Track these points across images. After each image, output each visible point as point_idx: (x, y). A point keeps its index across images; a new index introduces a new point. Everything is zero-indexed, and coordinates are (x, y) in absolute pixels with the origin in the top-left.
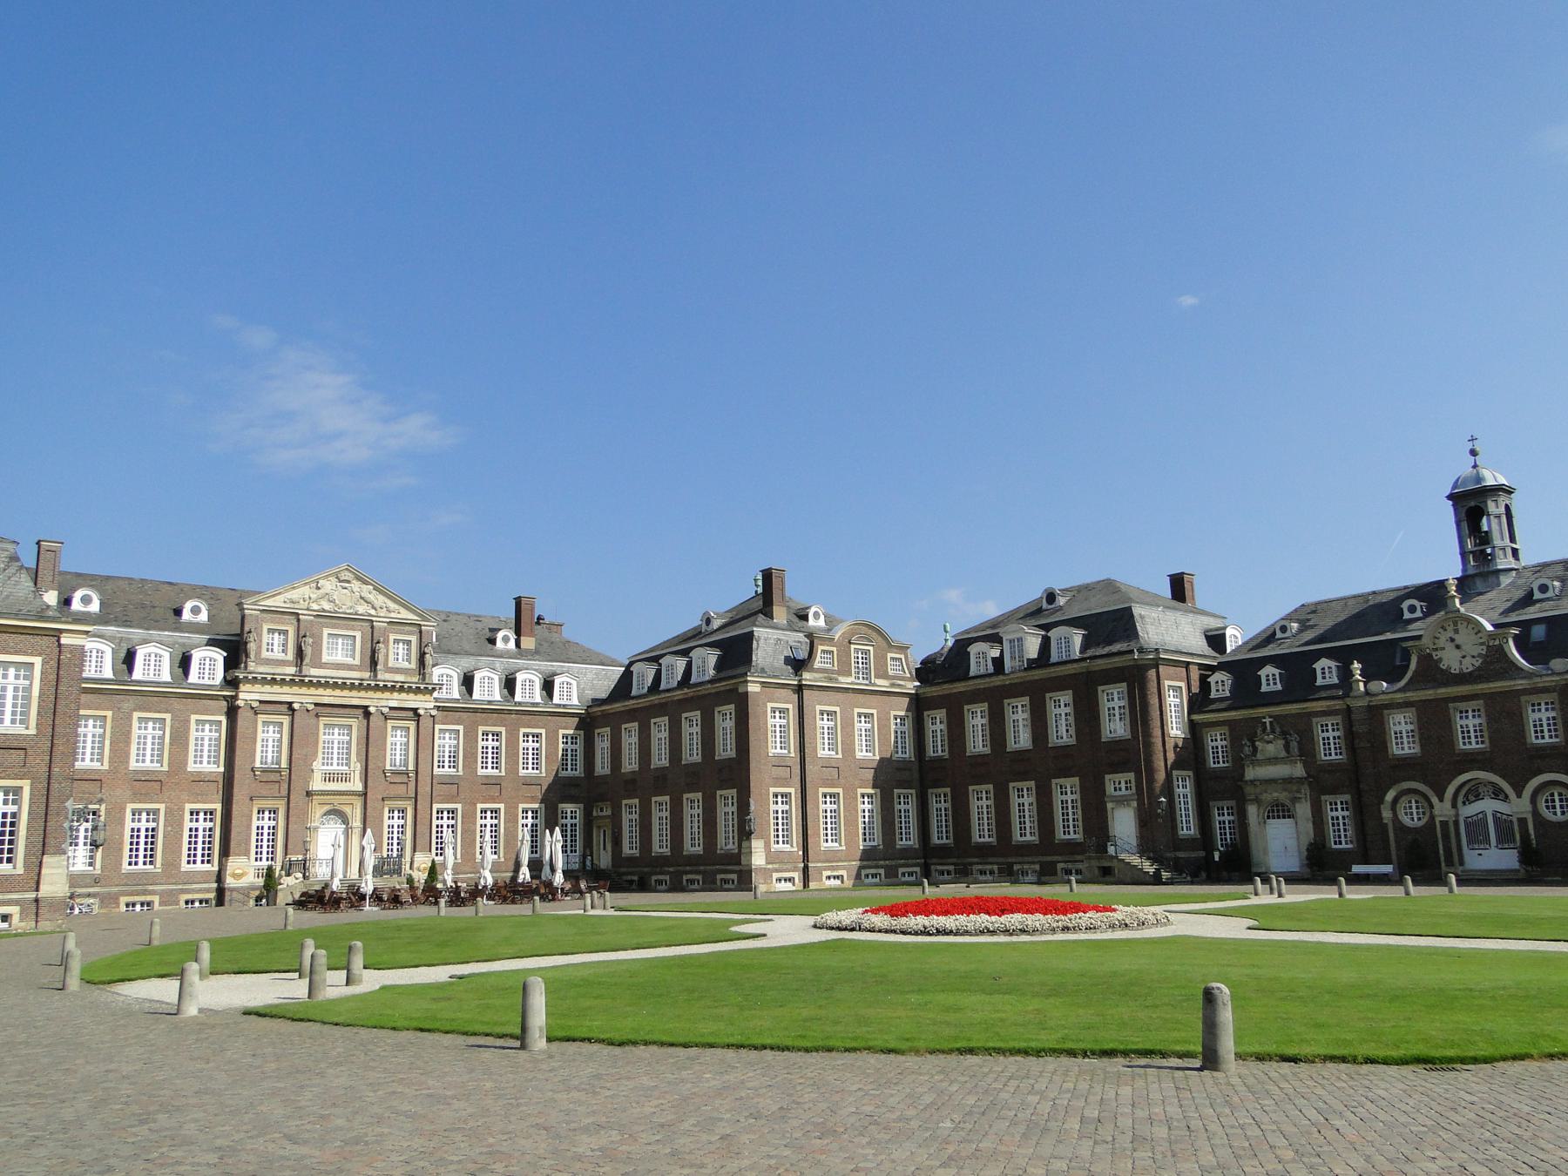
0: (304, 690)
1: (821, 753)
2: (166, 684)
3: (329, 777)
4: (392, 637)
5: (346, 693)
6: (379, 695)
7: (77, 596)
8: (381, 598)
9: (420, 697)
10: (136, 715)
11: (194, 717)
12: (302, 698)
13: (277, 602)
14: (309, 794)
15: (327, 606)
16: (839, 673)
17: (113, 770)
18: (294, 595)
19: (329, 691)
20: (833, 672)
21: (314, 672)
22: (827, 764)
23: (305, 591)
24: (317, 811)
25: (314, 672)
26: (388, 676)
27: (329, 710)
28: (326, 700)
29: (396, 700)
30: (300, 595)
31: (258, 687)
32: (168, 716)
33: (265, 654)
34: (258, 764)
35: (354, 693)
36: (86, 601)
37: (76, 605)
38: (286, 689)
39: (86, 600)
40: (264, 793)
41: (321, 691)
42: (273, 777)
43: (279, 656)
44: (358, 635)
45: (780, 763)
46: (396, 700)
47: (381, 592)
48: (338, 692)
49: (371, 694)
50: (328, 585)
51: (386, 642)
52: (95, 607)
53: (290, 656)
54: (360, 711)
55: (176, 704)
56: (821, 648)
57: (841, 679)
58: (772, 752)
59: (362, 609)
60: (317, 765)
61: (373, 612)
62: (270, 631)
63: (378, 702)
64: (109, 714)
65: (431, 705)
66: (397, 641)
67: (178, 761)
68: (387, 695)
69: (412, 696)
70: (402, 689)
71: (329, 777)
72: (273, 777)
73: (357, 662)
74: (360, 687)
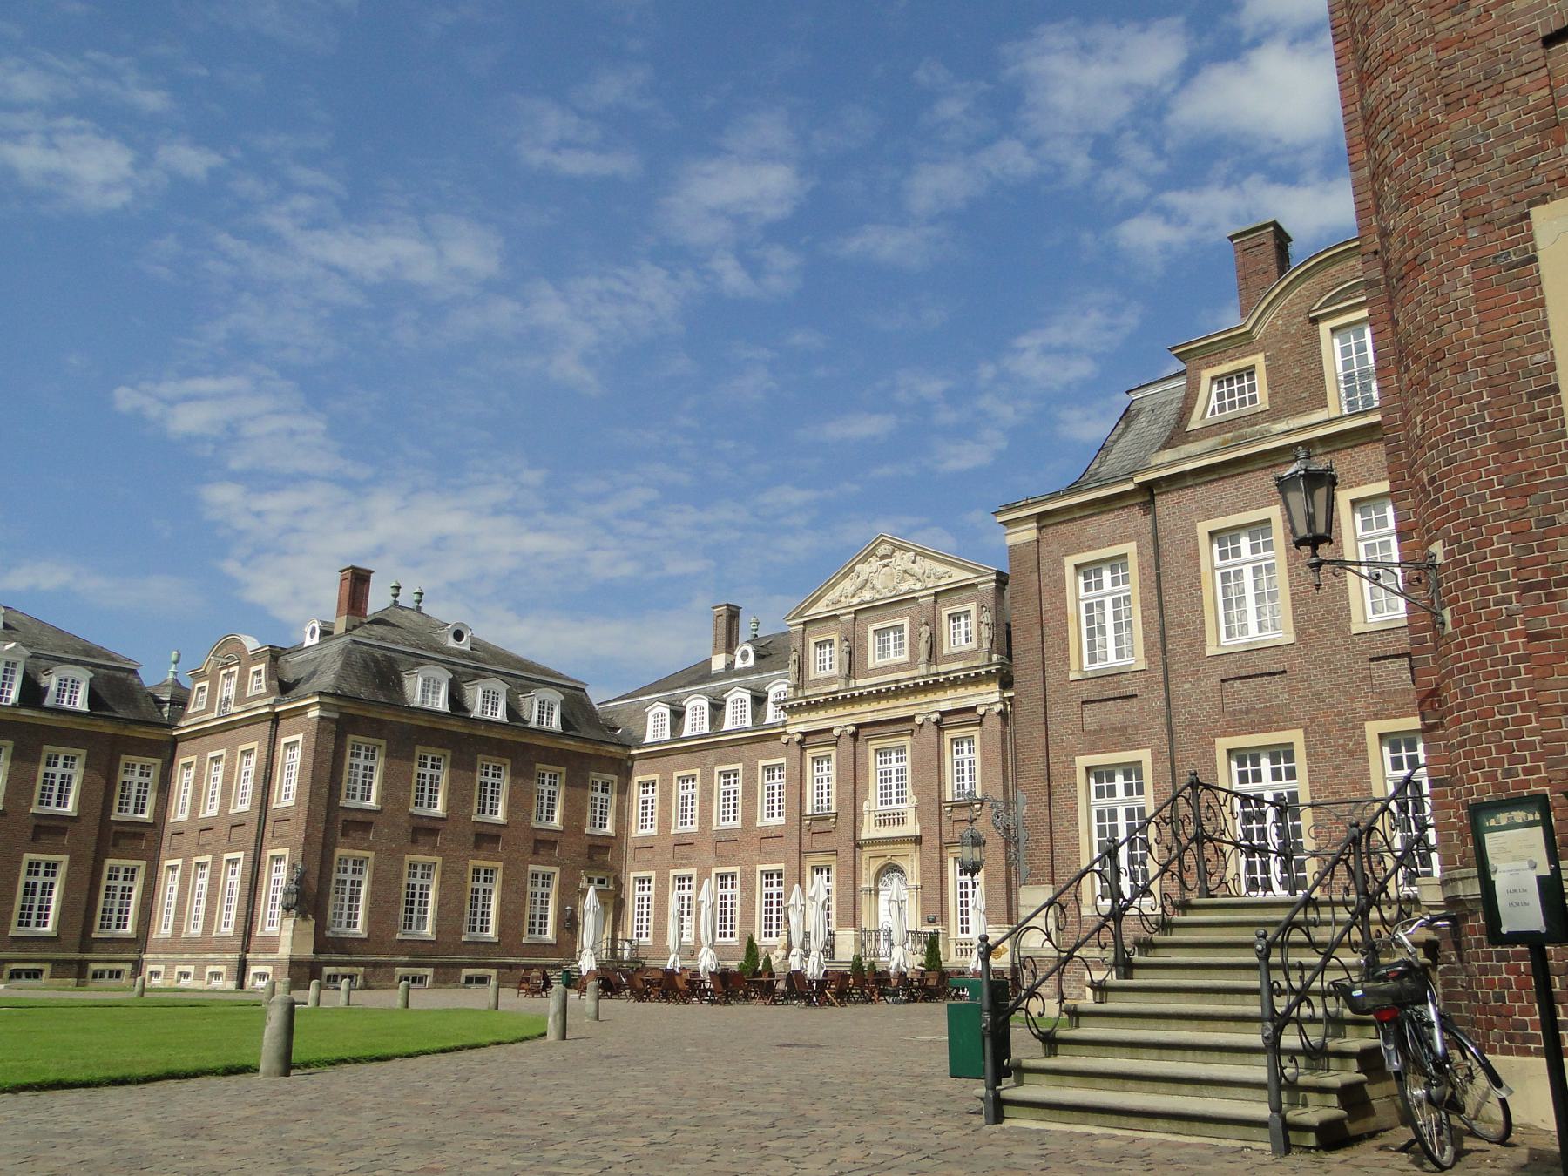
0: (849, 710)
1: (1220, 641)
2: (746, 730)
3: (884, 820)
4: (945, 613)
5: (893, 703)
6: (931, 697)
7: (738, 653)
8: (928, 564)
9: (983, 688)
10: (718, 769)
11: (761, 763)
12: (840, 720)
13: (819, 609)
14: (858, 845)
15: (867, 595)
16: (1275, 414)
17: (702, 832)
18: (834, 594)
19: (875, 706)
20: (1253, 419)
21: (860, 683)
22: (1250, 669)
23: (847, 586)
24: (868, 870)
25: (860, 683)
26: (942, 668)
27: (879, 730)
28: (870, 718)
29: (948, 700)
30: (843, 594)
31: (805, 717)
32: (739, 766)
33: (813, 673)
34: (809, 812)
35: (903, 701)
36: (745, 657)
37: (739, 664)
38: (831, 713)
39: (745, 656)
40: (818, 846)
41: (866, 707)
42: (824, 826)
43: (827, 673)
44: (906, 622)
45: (1110, 690)
46: (948, 700)
47: (925, 556)
48: (884, 704)
49: (921, 698)
50: (864, 570)
51: (933, 623)
52: (751, 662)
53: (835, 671)
54: (909, 726)
55: (746, 750)
56: (1206, 375)
57: (1281, 426)
58: (1081, 664)
59: (904, 587)
60: (871, 804)
61: (918, 586)
62: (819, 645)
63: (926, 707)
64: (697, 772)
65: (996, 697)
66: (954, 617)
67: (749, 818)
68: (940, 695)
69: (971, 690)
70: (955, 683)
71: (884, 820)
72: (824, 826)
73: (905, 657)
74: (898, 692)
